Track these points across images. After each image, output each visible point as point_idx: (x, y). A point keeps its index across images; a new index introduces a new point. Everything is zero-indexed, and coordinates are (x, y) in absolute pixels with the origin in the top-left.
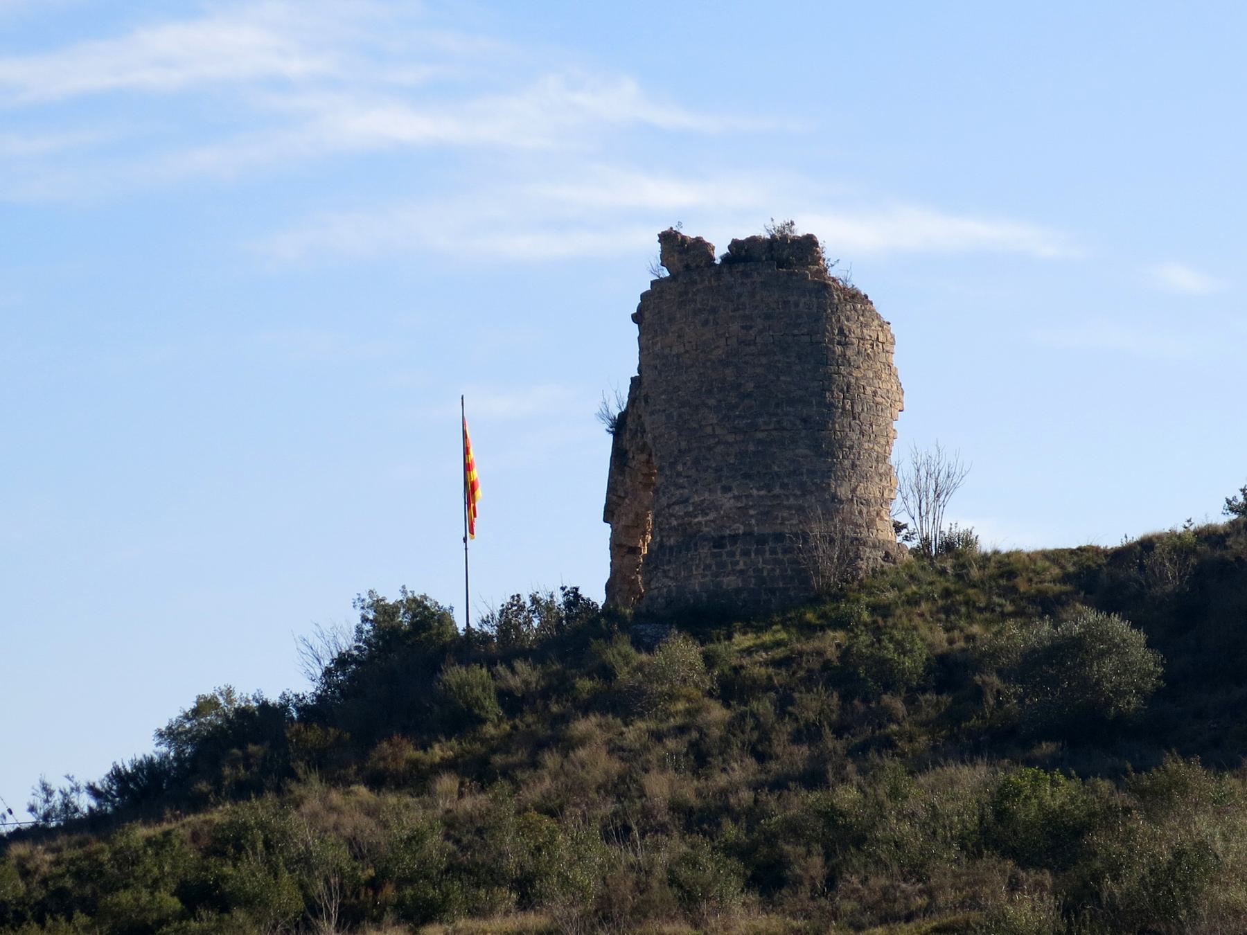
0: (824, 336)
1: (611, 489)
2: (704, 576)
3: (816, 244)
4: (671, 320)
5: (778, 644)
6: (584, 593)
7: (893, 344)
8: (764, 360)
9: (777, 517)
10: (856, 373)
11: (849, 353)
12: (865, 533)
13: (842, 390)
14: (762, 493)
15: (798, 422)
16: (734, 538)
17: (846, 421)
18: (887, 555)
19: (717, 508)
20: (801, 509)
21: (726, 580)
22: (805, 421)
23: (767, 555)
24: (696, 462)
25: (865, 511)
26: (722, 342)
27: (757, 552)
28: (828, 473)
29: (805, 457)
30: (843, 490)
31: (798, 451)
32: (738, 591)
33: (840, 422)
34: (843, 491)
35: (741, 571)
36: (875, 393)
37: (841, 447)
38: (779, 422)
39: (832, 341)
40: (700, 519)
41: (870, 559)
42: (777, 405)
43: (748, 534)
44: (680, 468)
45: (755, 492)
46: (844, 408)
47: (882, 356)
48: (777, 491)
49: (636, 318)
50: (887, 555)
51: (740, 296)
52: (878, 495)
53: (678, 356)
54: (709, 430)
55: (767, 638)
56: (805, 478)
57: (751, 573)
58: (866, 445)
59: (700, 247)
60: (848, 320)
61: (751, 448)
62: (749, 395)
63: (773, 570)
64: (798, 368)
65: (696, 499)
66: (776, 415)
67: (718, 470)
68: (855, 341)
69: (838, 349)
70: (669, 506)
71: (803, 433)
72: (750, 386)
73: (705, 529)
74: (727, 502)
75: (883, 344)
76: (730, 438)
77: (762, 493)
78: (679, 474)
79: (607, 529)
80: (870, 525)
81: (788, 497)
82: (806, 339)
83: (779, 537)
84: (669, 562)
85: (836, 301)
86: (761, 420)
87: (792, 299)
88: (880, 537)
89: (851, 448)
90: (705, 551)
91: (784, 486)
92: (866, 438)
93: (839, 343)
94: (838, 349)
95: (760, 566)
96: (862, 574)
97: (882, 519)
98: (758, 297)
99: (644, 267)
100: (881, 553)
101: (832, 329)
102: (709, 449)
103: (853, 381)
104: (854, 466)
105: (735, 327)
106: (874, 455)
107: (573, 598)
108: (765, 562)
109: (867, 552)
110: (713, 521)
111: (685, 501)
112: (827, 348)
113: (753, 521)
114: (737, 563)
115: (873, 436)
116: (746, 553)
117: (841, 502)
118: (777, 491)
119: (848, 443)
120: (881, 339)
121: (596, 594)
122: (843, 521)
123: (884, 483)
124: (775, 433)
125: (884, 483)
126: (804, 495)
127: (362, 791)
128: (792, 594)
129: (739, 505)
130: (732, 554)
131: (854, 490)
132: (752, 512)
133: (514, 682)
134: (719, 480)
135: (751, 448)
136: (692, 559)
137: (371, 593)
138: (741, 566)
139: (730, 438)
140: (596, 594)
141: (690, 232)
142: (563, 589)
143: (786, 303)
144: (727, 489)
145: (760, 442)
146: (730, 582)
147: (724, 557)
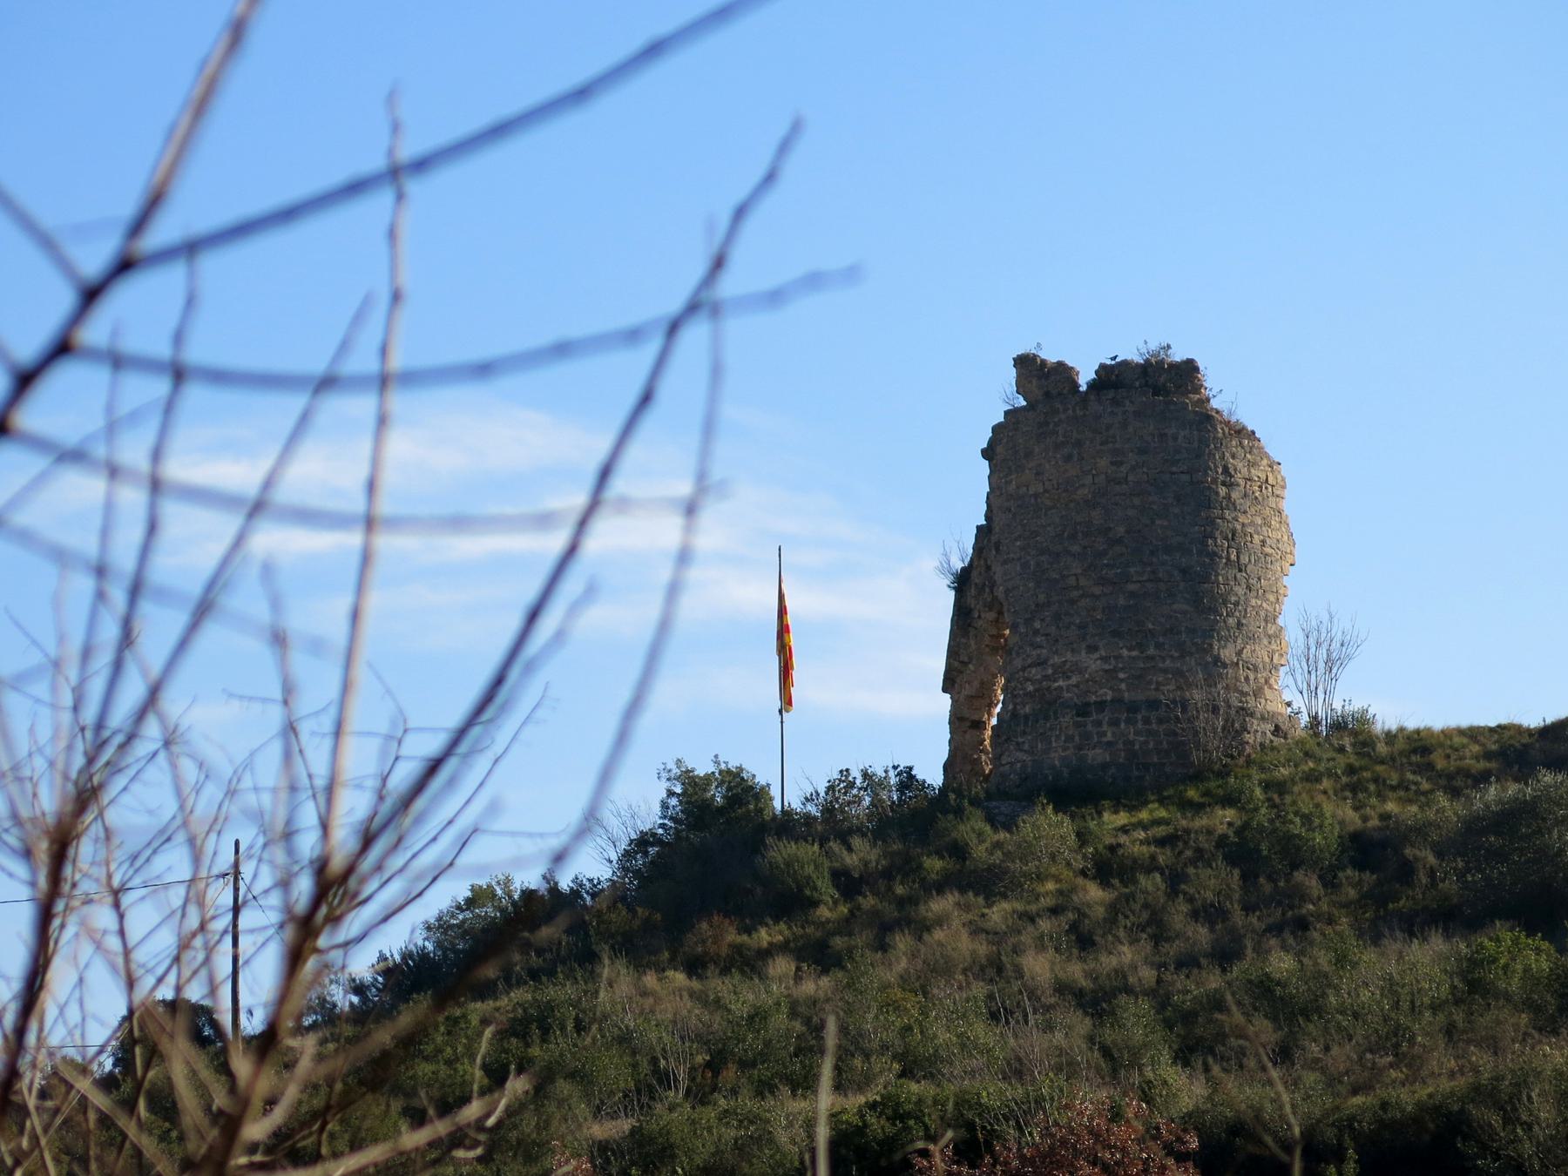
0: (1206, 474)
1: (952, 653)
2: (1065, 749)
3: (1197, 369)
4: (1029, 455)
5: (1158, 822)
6: (919, 774)
7: (1284, 487)
8: (1136, 501)
9: (1150, 683)
11: (1235, 495)
12: (1251, 700)
13: (1226, 538)
14: (1134, 653)
15: (1176, 573)
16: (1101, 706)
17: (1232, 572)
18: (1277, 728)
19: (1081, 672)
20: (1179, 673)
21: (1091, 754)
22: (1184, 571)
23: (1140, 726)
24: (1057, 617)
25: (1252, 677)
26: (1088, 480)
27: (1128, 721)
28: (1210, 632)
29: (1184, 613)
31: (1175, 607)
32: (1105, 766)
33: (1223, 574)
34: (1228, 654)
35: (1109, 744)
36: (1263, 542)
37: (1225, 603)
38: (1153, 572)
39: (1215, 481)
40: (1061, 683)
41: (1258, 732)
42: (1152, 553)
43: (1118, 701)
44: (1037, 625)
45: (1125, 652)
46: (1228, 559)
47: (1272, 501)
48: (1151, 651)
49: (987, 453)
50: (1277, 728)
51: (1109, 427)
52: (1267, 660)
53: (1036, 496)
54: (1072, 581)
55: (1144, 815)
57: (1121, 746)
58: (1253, 602)
59: (1063, 372)
60: (1233, 457)
61: (1121, 601)
62: (1119, 541)
63: (1146, 742)
64: (1176, 511)
65: (1057, 660)
67: (1082, 627)
68: (1242, 482)
69: (1223, 491)
70: (1024, 669)
71: (1182, 585)
72: (1121, 530)
73: (1066, 695)
74: (1093, 663)
75: (1271, 486)
76: (1097, 591)
77: (1134, 653)
78: (1036, 632)
79: (946, 700)
80: (1258, 693)
81: (1163, 659)
82: (1185, 478)
83: (1154, 704)
84: (1024, 733)
86: (1132, 570)
89: (1237, 604)
90: (1067, 720)
91: (1159, 646)
92: (1254, 593)
93: (1224, 484)
94: (1223, 491)
95: (1131, 737)
96: (1248, 750)
97: (1271, 687)
98: (1131, 429)
99: (997, 395)
100: (1270, 727)
102: (1072, 602)
103: (1239, 527)
104: (1239, 625)
105: (1103, 463)
106: (1262, 614)
107: (908, 779)
108: (1137, 733)
109: (1255, 724)
110: (1077, 686)
111: (1042, 663)
113: (1123, 686)
114: (1105, 734)
116: (1114, 723)
117: (1225, 666)
119: (1233, 599)
120: (1271, 481)
121: (932, 774)
122: (1227, 688)
123: (1274, 647)
124: (1149, 585)
125: (1274, 647)
126: (1182, 656)
127: (679, 977)
128: (1168, 769)
129: (1107, 667)
130: (1099, 723)
131: (1239, 653)
132: (1121, 675)
133: (851, 860)
134: (1084, 639)
135: (1121, 601)
136: (1051, 729)
137: (679, 762)
138: (1109, 737)
139: (1097, 591)
140: (932, 774)
141: (1051, 356)
142: (895, 768)
143: (1163, 436)
144: (1092, 649)
145: (1133, 594)
146: (1096, 755)
147: (1089, 728)
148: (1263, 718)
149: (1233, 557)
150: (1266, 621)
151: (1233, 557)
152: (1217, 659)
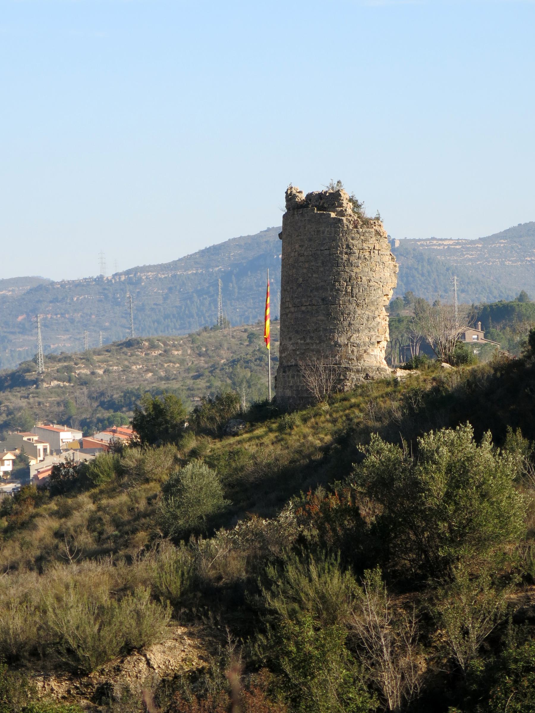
0: (337, 250)
8: (307, 265)
10: (355, 270)
11: (351, 259)
12: (355, 363)
13: (346, 281)
17: (347, 298)
20: (318, 351)
22: (323, 300)
28: (332, 331)
29: (322, 321)
30: (342, 338)
31: (319, 318)
32: (289, 398)
34: (342, 340)
35: (291, 386)
36: (369, 281)
37: (342, 314)
38: (311, 301)
42: (311, 291)
45: (299, 341)
46: (346, 291)
48: (308, 341)
52: (367, 340)
56: (321, 333)
57: (295, 388)
58: (359, 312)
64: (322, 269)
66: (310, 297)
68: (357, 251)
69: (345, 257)
76: (292, 309)
77: (302, 342)
81: (312, 344)
82: (327, 252)
85: (345, 229)
86: (303, 300)
87: (321, 229)
88: (366, 364)
89: (349, 314)
91: (311, 338)
93: (346, 253)
94: (345, 257)
96: (346, 389)
97: (368, 354)
100: (362, 376)
101: (342, 245)
103: (353, 274)
104: (350, 324)
106: (365, 317)
109: (352, 375)
112: (338, 256)
115: (365, 306)
116: (293, 377)
117: (340, 346)
118: (308, 341)
119: (347, 312)
120: (377, 248)
122: (341, 357)
124: (309, 307)
126: (320, 343)
127: (18, 530)
129: (294, 348)
131: (349, 339)
138: (291, 384)
139: (292, 309)
143: (318, 231)
145: (303, 312)
146: (288, 393)
148: (358, 371)
149: (349, 290)
150: (368, 320)
151: (349, 290)
152: (336, 343)
